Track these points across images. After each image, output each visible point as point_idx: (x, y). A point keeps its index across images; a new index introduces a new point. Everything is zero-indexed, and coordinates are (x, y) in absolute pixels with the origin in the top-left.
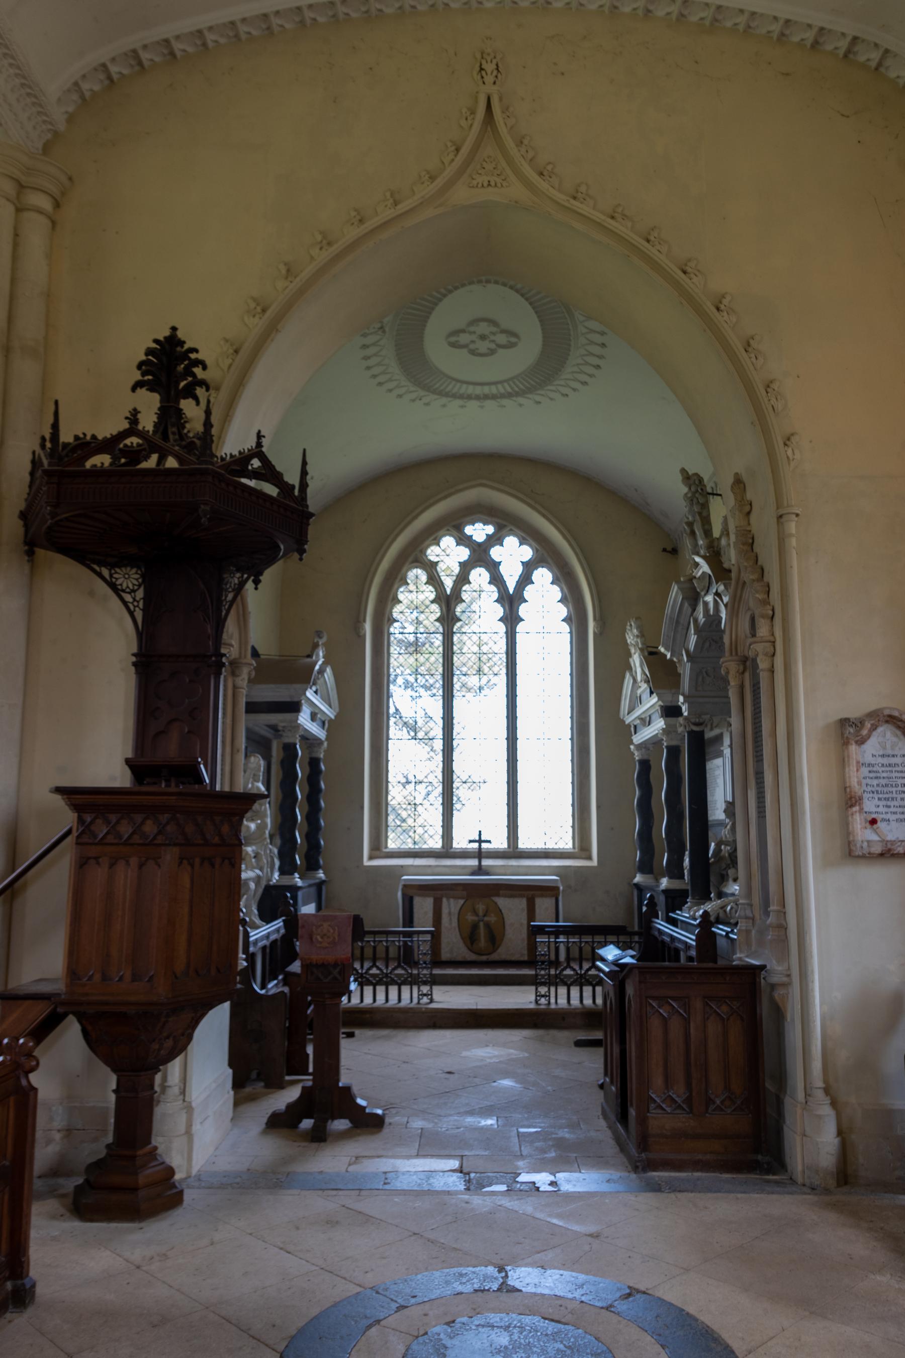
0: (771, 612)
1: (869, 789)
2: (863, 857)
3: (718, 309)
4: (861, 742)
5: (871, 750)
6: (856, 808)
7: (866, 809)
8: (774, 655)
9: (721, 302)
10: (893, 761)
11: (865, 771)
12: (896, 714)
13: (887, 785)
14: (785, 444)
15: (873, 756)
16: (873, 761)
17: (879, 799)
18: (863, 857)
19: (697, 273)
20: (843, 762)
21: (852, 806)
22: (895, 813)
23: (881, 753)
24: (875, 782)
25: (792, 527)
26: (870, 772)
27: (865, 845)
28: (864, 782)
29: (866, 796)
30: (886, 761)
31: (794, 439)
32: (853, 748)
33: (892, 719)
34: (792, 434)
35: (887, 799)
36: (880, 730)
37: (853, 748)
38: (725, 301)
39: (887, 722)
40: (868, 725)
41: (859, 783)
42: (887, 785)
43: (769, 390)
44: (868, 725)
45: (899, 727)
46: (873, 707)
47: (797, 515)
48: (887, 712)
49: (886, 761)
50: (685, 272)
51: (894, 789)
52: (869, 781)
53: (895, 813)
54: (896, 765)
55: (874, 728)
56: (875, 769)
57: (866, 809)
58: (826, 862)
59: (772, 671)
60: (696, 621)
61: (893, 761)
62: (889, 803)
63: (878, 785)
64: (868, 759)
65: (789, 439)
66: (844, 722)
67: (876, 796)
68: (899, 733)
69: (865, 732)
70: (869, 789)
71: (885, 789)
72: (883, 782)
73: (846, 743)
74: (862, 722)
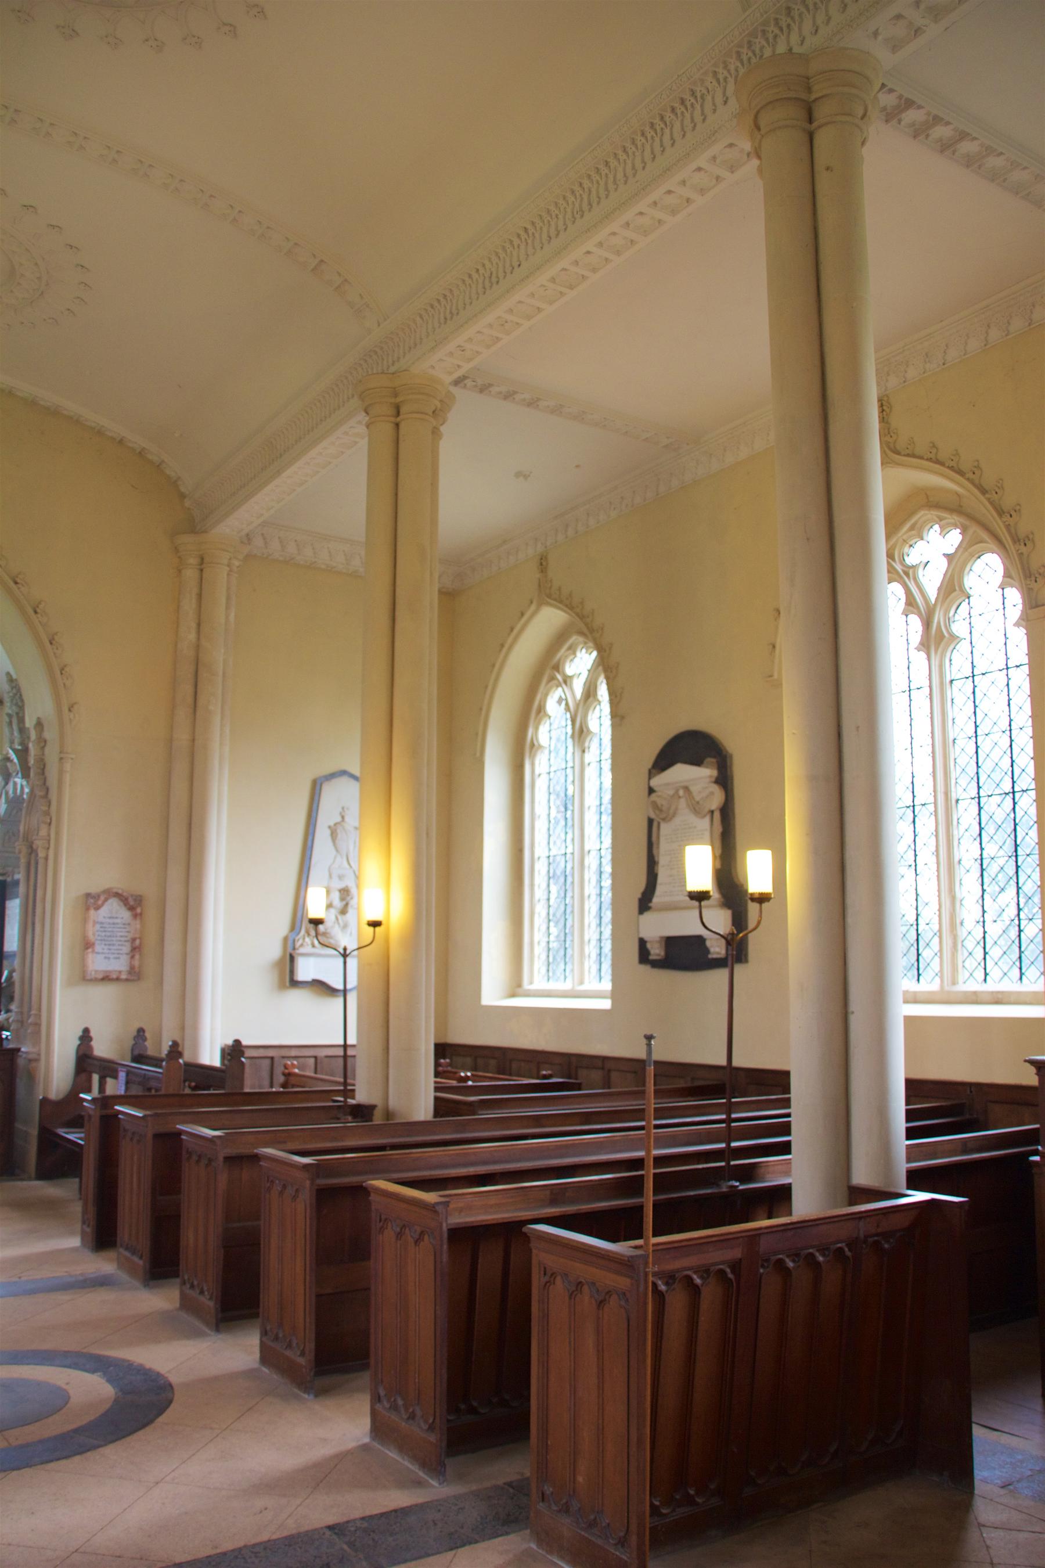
0: (49, 821)
1: (99, 938)
2: (91, 980)
3: (36, 612)
4: (97, 908)
5: (104, 911)
6: (90, 950)
7: (96, 950)
8: (48, 848)
9: (38, 607)
10: (116, 921)
11: (98, 926)
12: (120, 891)
13: (110, 936)
14: (70, 710)
15: (104, 917)
16: (104, 920)
17: (105, 945)
18: (91, 980)
19: (23, 583)
20: (85, 920)
21: (87, 948)
22: (114, 954)
23: (109, 916)
24: (103, 934)
25: (68, 766)
26: (101, 927)
27: (93, 973)
28: (97, 933)
29: (97, 942)
30: (111, 921)
31: (76, 707)
32: (92, 912)
33: (117, 895)
34: (75, 703)
35: (110, 945)
36: (110, 901)
37: (92, 912)
38: (41, 606)
39: (114, 896)
40: (102, 898)
41: (94, 935)
42: (110, 936)
43: (63, 672)
44: (102, 898)
45: (121, 900)
46: (107, 886)
47: (72, 759)
48: (115, 890)
49: (111, 921)
50: (16, 583)
51: (114, 939)
52: (100, 933)
53: (114, 954)
54: (117, 924)
55: (106, 900)
56: (104, 926)
57: (96, 950)
58: (70, 983)
59: (46, 858)
60: (7, 793)
61: (116, 921)
62: (111, 947)
63: (105, 936)
64: (101, 919)
65: (72, 707)
66: (88, 895)
67: (103, 942)
68: (122, 904)
69: (100, 902)
70: (99, 938)
71: (110, 939)
72: (108, 934)
73: (88, 909)
74: (99, 896)
